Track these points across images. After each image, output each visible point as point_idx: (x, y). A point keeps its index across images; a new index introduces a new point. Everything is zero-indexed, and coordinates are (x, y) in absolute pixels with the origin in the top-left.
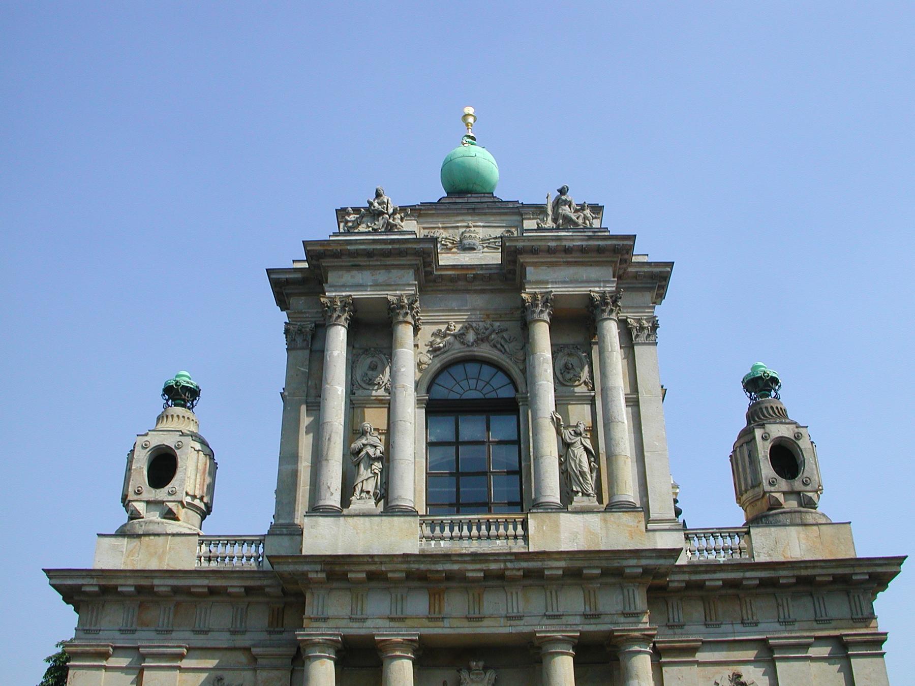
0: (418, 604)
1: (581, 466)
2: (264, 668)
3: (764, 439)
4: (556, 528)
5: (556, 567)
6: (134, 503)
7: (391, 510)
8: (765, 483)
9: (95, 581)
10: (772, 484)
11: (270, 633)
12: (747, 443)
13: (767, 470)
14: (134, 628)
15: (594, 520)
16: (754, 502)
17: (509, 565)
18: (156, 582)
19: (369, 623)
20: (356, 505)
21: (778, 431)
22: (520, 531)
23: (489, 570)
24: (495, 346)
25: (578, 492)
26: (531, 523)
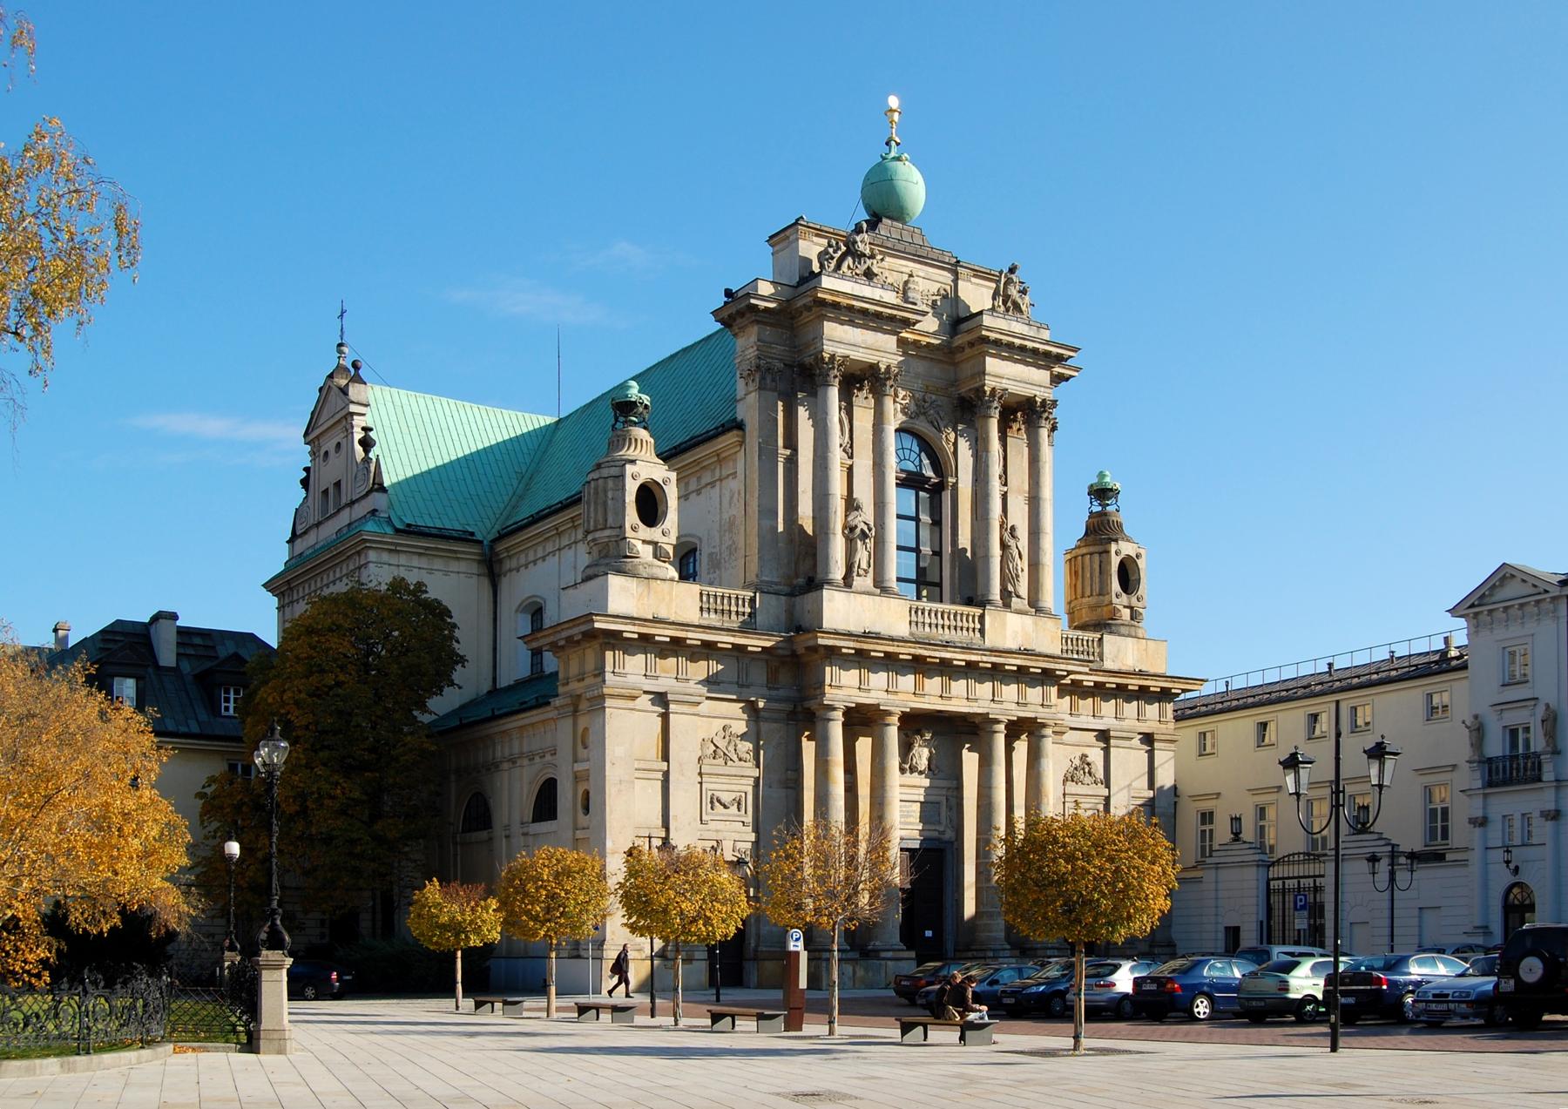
0: (907, 682)
1: (1017, 570)
2: (766, 720)
3: (1117, 553)
4: (1004, 625)
5: (1012, 663)
6: (631, 540)
7: (881, 586)
8: (1114, 596)
9: (636, 629)
10: (1117, 596)
11: (770, 689)
12: (1100, 553)
13: (1115, 586)
14: (658, 674)
15: (1028, 621)
16: (1093, 608)
17: (985, 659)
18: (690, 635)
19: (873, 694)
20: (858, 582)
21: (1126, 549)
22: (978, 626)
23: (971, 661)
24: (932, 423)
25: (1010, 592)
26: (987, 618)
